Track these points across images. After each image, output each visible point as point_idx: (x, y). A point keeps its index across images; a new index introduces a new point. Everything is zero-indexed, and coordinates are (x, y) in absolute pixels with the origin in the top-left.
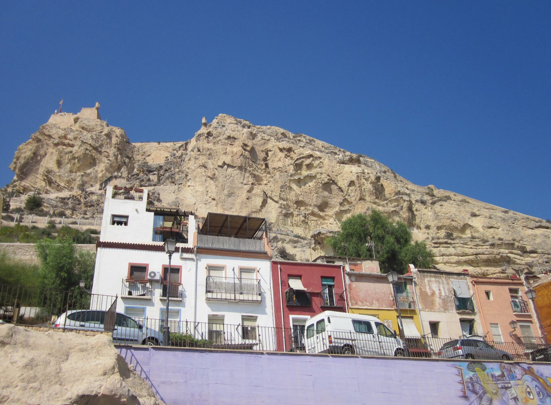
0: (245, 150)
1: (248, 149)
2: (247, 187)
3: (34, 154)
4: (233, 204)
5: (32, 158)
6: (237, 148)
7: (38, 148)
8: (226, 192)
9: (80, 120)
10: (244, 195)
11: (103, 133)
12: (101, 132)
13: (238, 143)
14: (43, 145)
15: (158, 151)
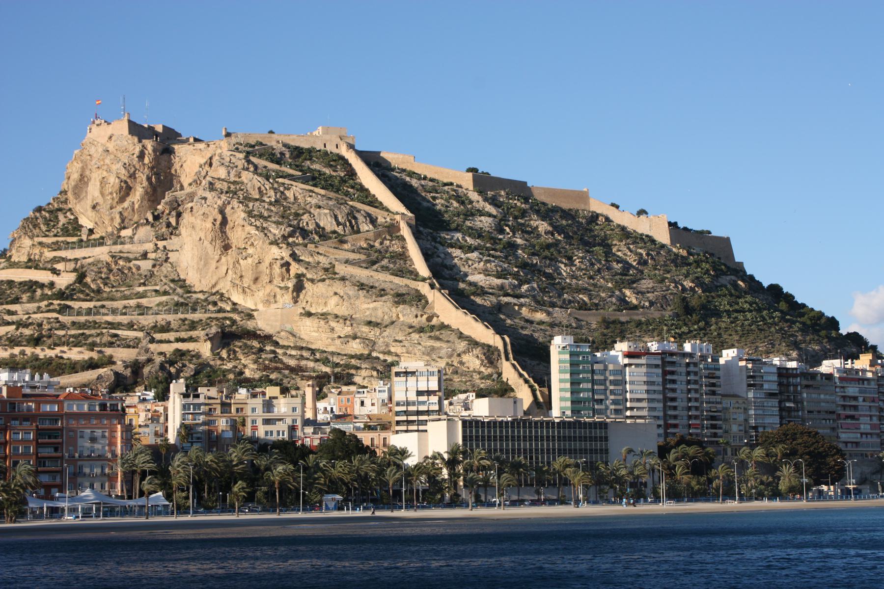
0: (214, 225)
1: (218, 223)
2: (217, 257)
3: (81, 175)
4: (207, 273)
5: (80, 180)
6: (209, 225)
7: (83, 169)
8: (202, 262)
9: (113, 138)
10: (214, 264)
11: (135, 156)
12: (133, 154)
13: (211, 219)
14: (86, 165)
15: (193, 156)
